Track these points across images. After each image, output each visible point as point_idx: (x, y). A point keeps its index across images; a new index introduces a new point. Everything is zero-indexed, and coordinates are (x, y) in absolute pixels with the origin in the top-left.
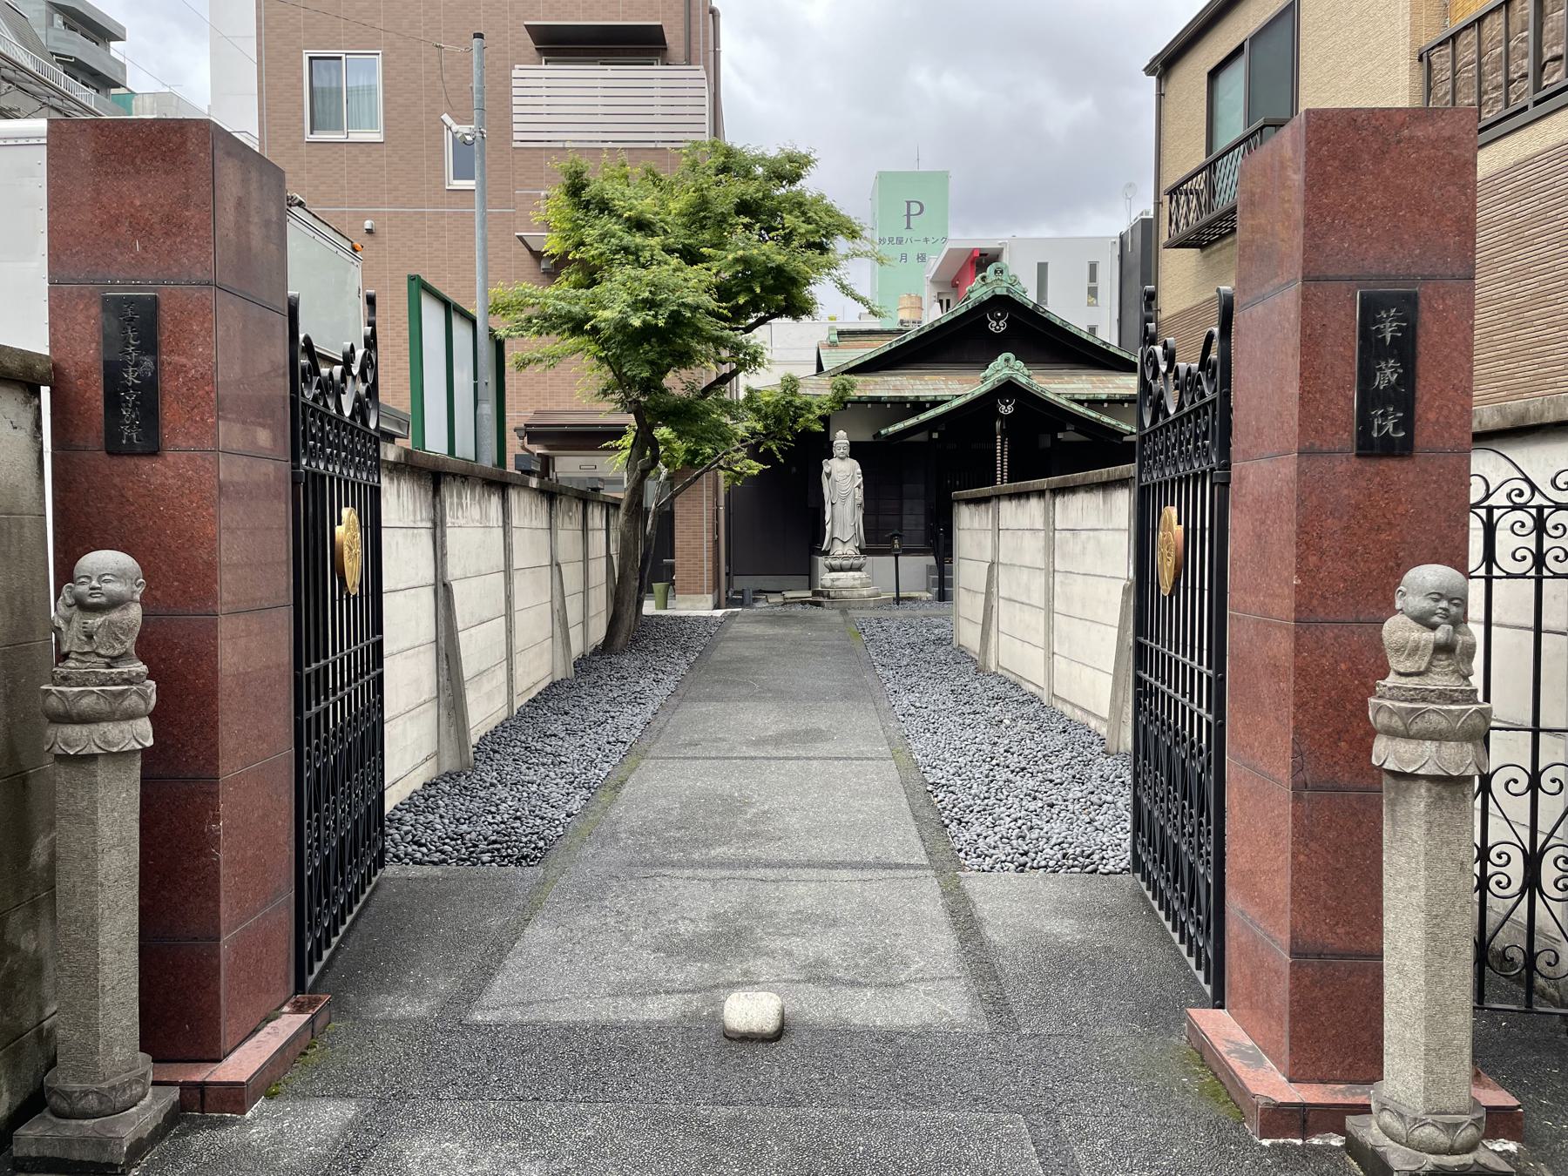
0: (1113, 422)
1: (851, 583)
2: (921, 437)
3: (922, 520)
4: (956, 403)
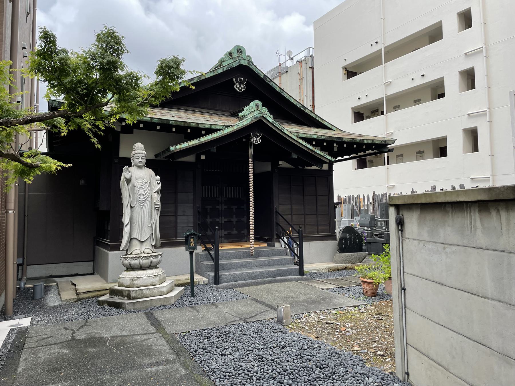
0: (322, 153)
1: (151, 280)
2: (191, 158)
3: (191, 219)
4: (227, 131)
